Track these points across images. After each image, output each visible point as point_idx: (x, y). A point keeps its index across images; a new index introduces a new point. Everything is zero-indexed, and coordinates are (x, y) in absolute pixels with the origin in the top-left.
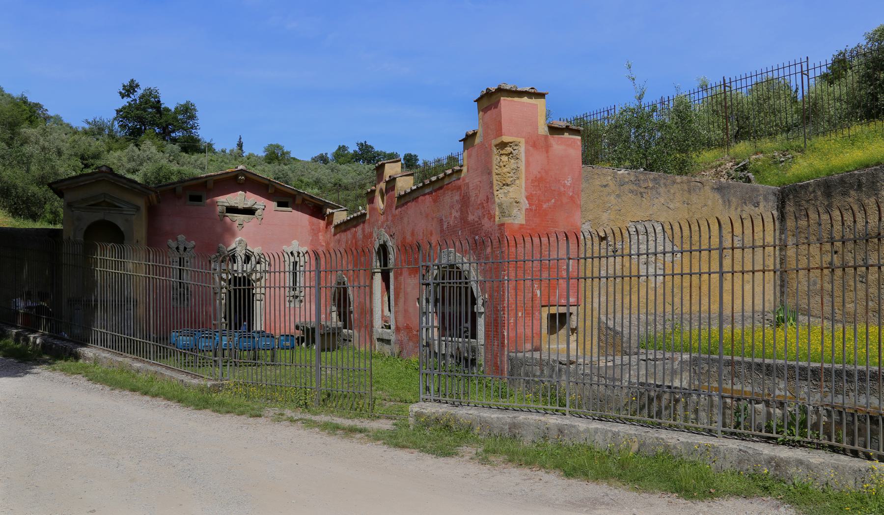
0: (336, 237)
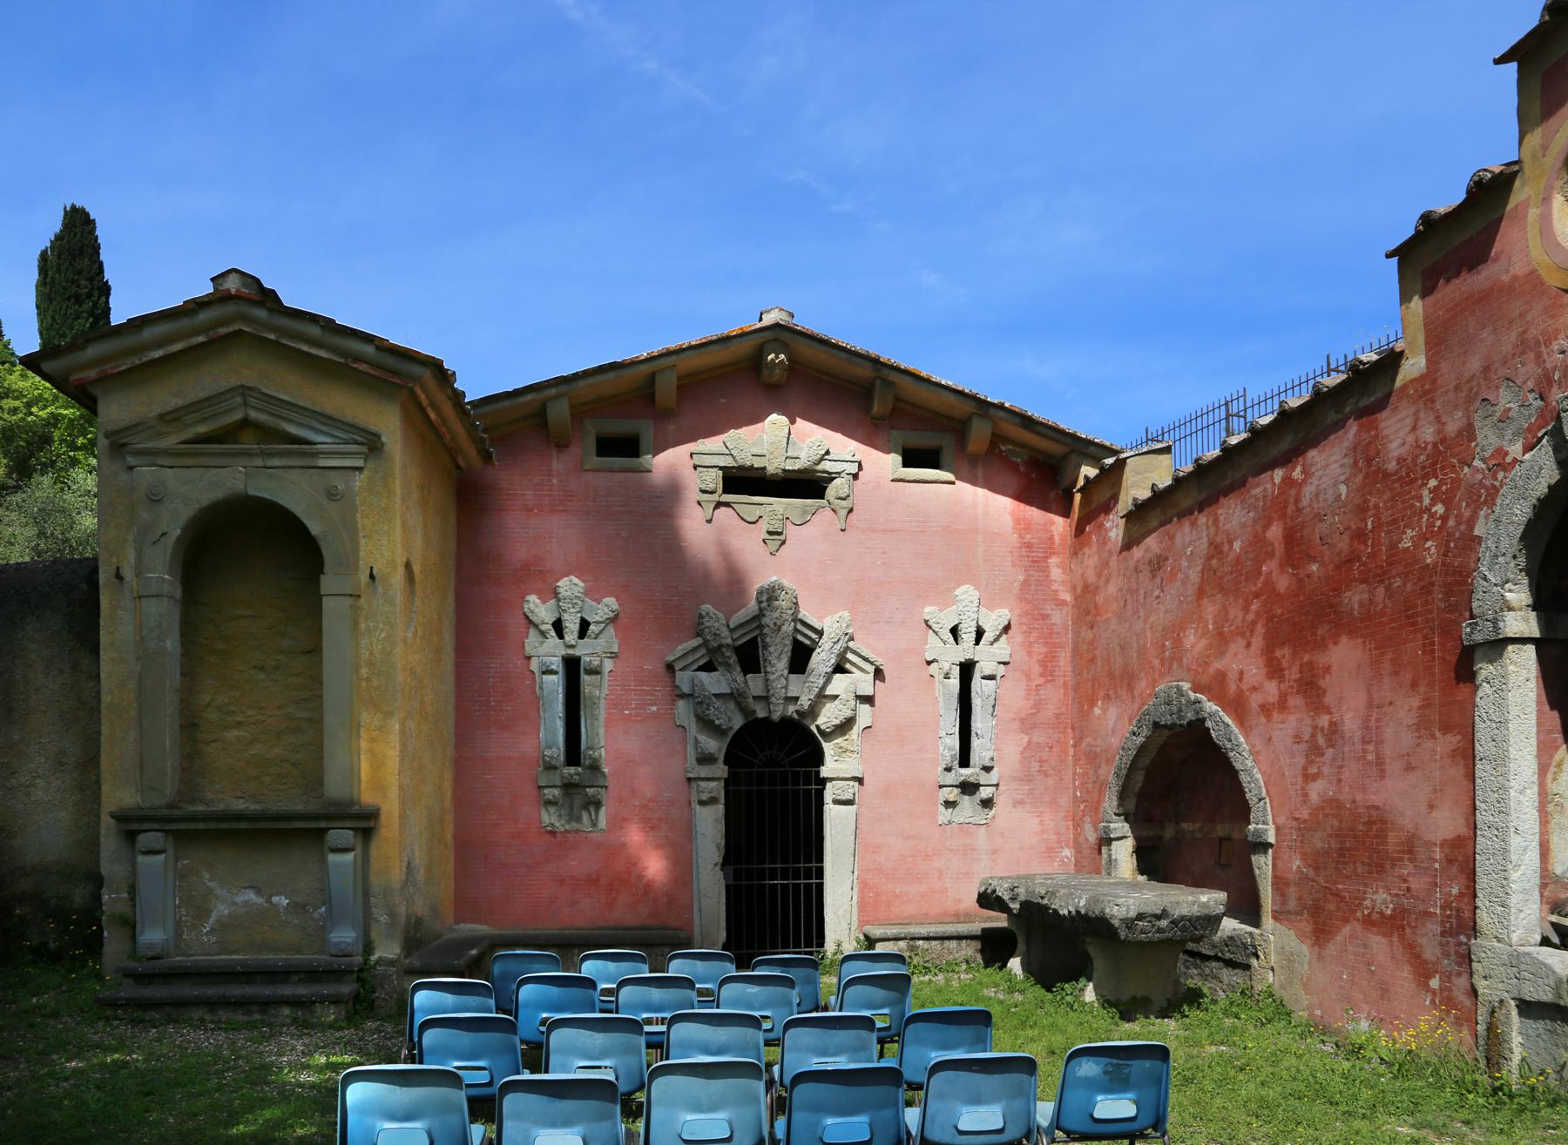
0: (1137, 553)
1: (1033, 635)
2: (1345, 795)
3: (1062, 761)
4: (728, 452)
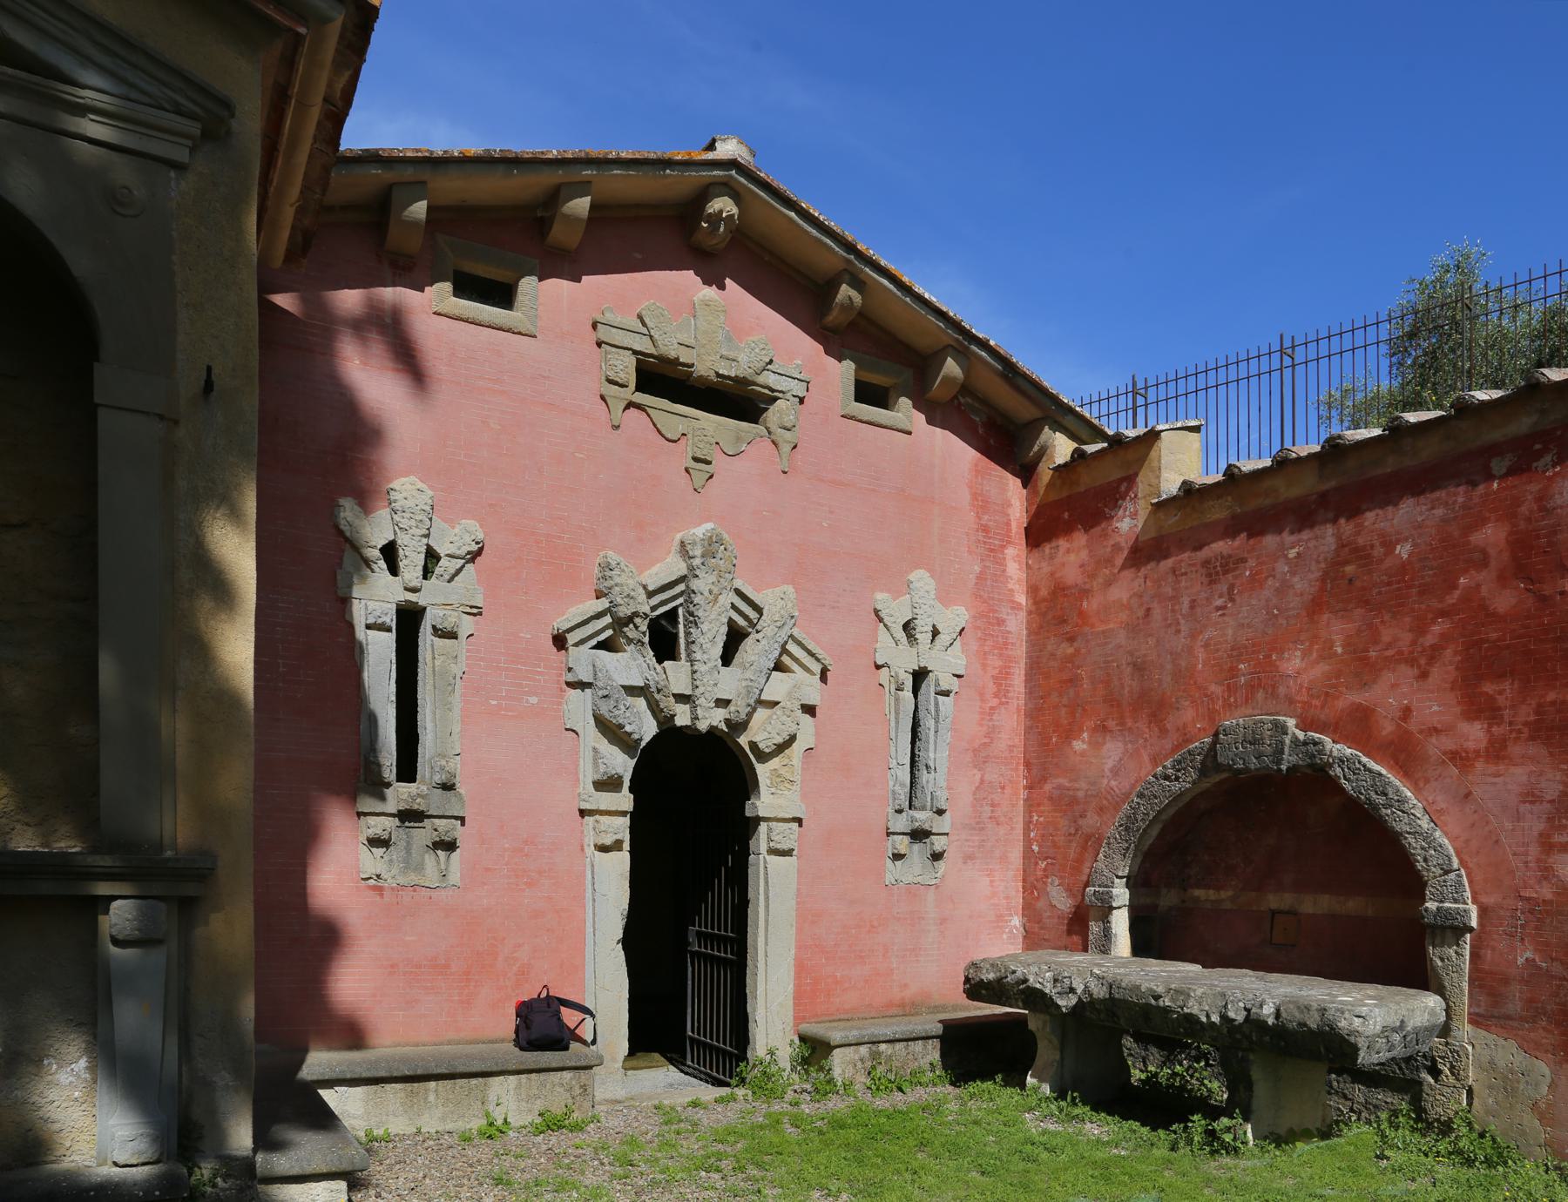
1: (988, 643)
3: (1013, 806)
4: (644, 331)
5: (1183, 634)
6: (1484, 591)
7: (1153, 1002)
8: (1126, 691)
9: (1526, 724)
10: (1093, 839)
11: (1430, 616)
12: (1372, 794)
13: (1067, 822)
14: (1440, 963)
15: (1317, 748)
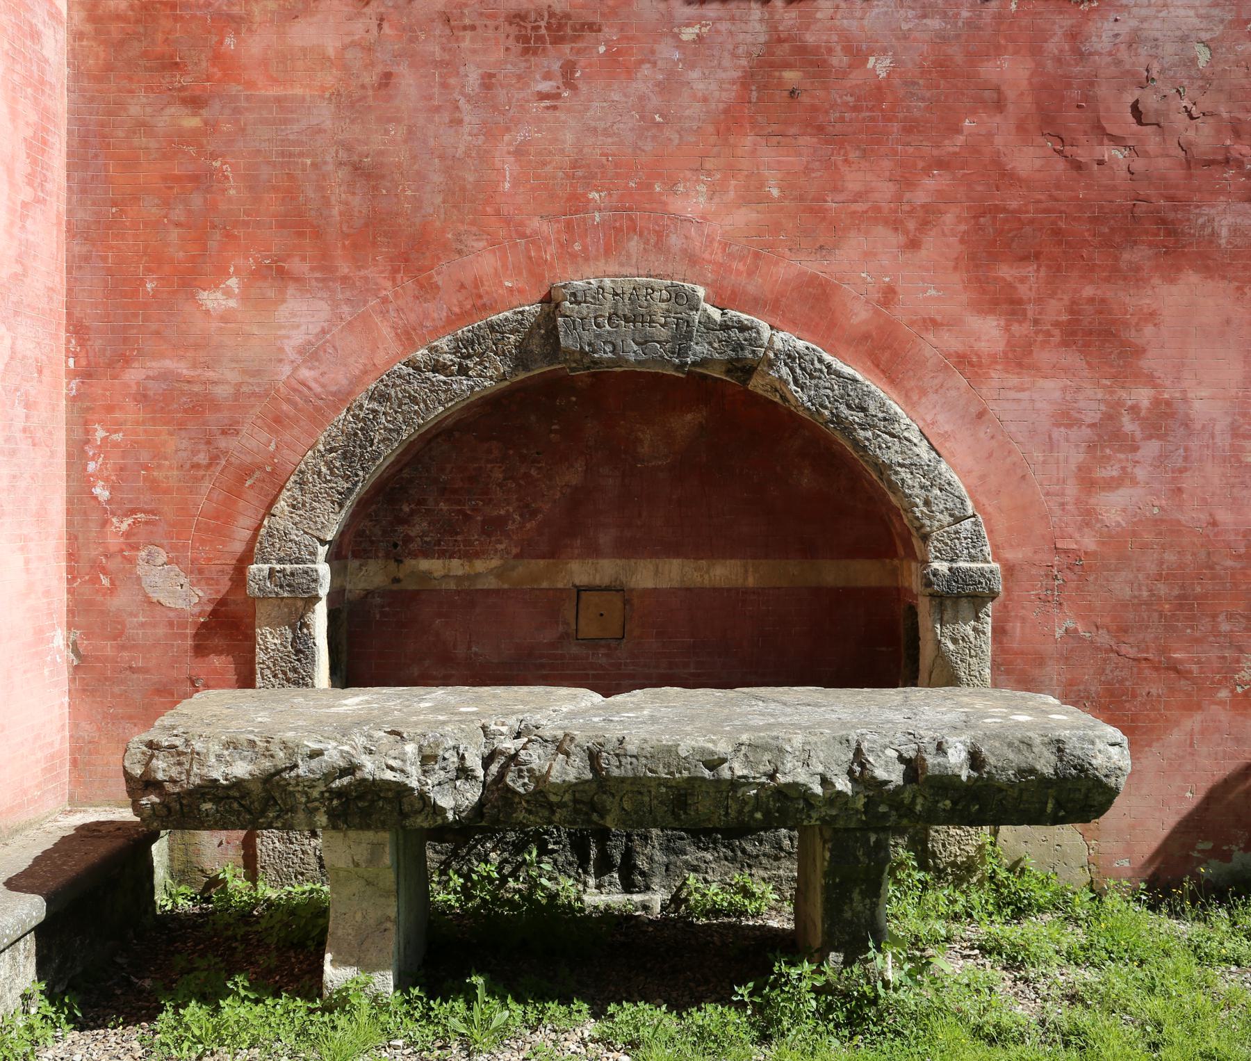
2: (1192, 515)
5: (466, 129)
6: (999, 140)
7: (707, 773)
8: (335, 211)
9: (1056, 324)
10: (257, 474)
11: (921, 164)
12: (843, 408)
13: (185, 444)
14: (951, 647)
15: (746, 334)
